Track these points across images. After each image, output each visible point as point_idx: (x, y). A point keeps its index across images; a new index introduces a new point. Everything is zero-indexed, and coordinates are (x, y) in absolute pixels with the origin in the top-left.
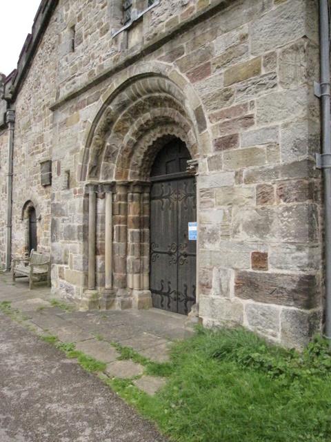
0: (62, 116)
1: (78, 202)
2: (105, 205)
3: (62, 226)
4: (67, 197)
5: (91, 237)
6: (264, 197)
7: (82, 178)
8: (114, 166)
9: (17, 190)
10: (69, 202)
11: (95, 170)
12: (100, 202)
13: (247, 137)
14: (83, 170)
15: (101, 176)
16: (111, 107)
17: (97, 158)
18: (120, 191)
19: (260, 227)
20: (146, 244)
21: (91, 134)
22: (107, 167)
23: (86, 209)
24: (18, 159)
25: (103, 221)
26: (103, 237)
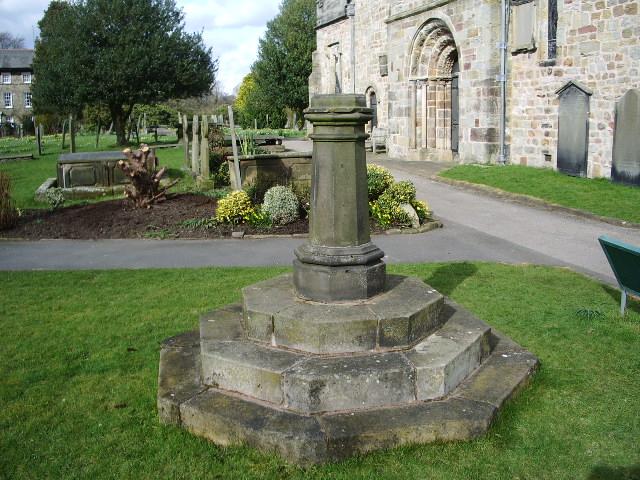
0: (394, 28)
1: (404, 90)
2: (421, 93)
3: (394, 107)
4: (398, 87)
5: (413, 114)
6: (478, 94)
7: (407, 75)
8: (427, 67)
9: (359, 77)
10: (399, 91)
11: (415, 69)
12: (418, 91)
13: (474, 64)
14: (407, 70)
15: (419, 73)
16: (422, 31)
17: (416, 62)
18: (431, 84)
19: (477, 108)
20: (449, 119)
21: (411, 48)
22: (422, 68)
23: (409, 96)
24: (359, 49)
25: (421, 104)
26: (421, 114)
